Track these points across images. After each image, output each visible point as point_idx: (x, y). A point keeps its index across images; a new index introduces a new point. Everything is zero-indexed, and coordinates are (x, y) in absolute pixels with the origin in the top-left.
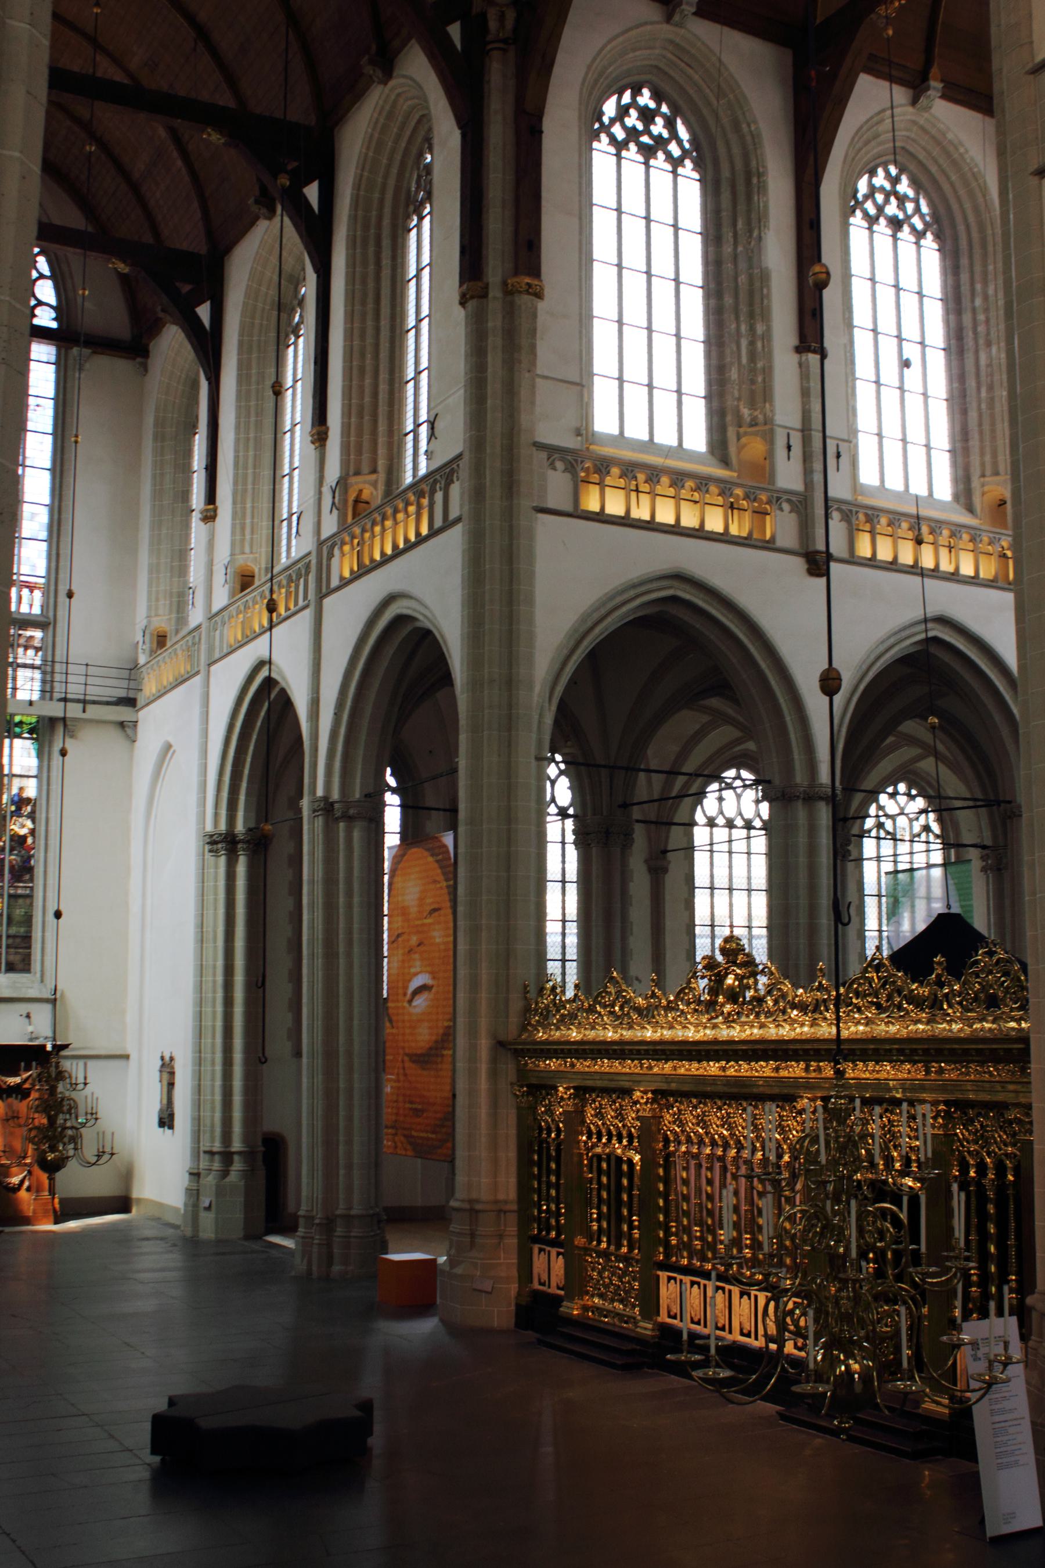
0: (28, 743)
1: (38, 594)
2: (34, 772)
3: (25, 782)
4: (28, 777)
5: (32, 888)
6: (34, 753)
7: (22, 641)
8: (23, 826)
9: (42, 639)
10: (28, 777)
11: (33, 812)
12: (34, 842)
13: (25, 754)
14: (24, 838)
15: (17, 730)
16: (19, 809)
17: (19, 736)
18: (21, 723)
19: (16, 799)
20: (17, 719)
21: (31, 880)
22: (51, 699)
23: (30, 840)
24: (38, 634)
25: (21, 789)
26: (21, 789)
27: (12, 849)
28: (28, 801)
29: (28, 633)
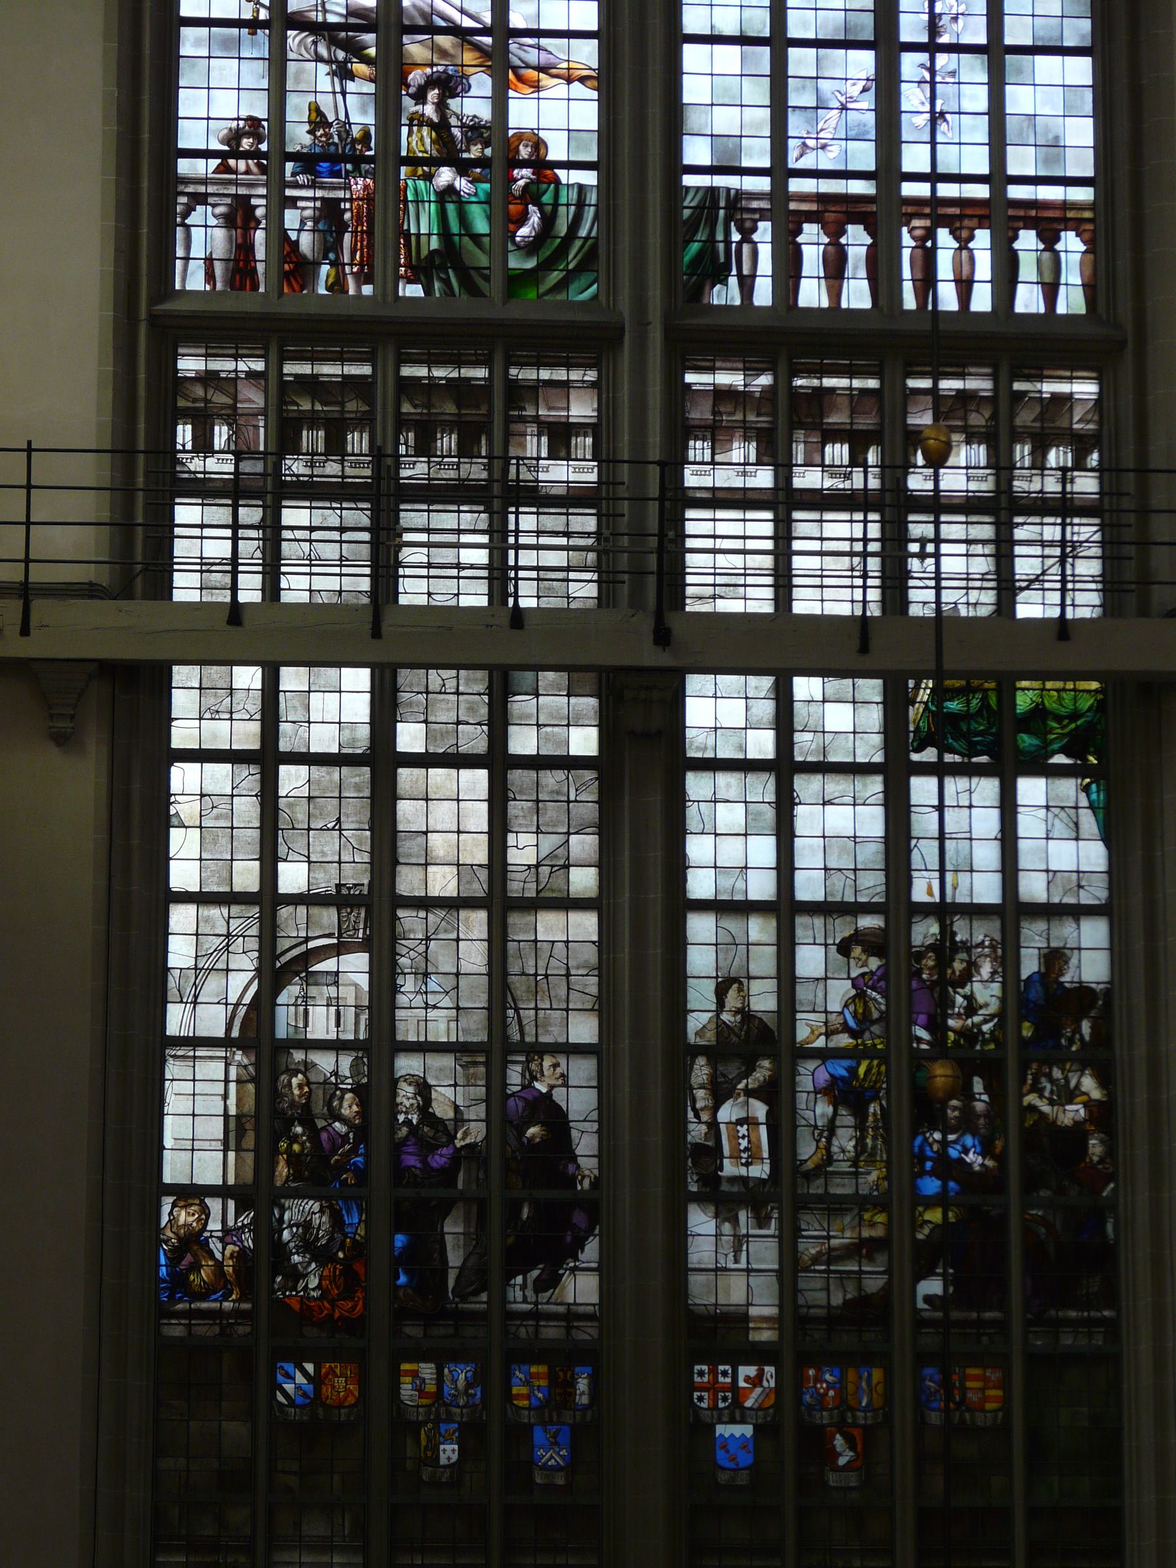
0: (1068, 788)
1: (1071, 244)
2: (1095, 893)
3: (1065, 932)
4: (1078, 912)
5: (1112, 1328)
6: (1089, 823)
7: (1026, 417)
8: (1068, 1095)
9: (1099, 402)
10: (1078, 912)
11: (1102, 1037)
12: (1110, 1152)
13: (1059, 829)
14: (1078, 1133)
15: (1026, 741)
16: (1048, 1032)
17: (1039, 767)
18: (1039, 713)
19: (1036, 993)
20: (1023, 701)
21: (1111, 1297)
22: (1144, 611)
23: (1095, 1147)
24: (1085, 389)
25: (1055, 958)
26: (1055, 958)
27: (1030, 1184)
28: (1083, 991)
29: (1049, 388)
